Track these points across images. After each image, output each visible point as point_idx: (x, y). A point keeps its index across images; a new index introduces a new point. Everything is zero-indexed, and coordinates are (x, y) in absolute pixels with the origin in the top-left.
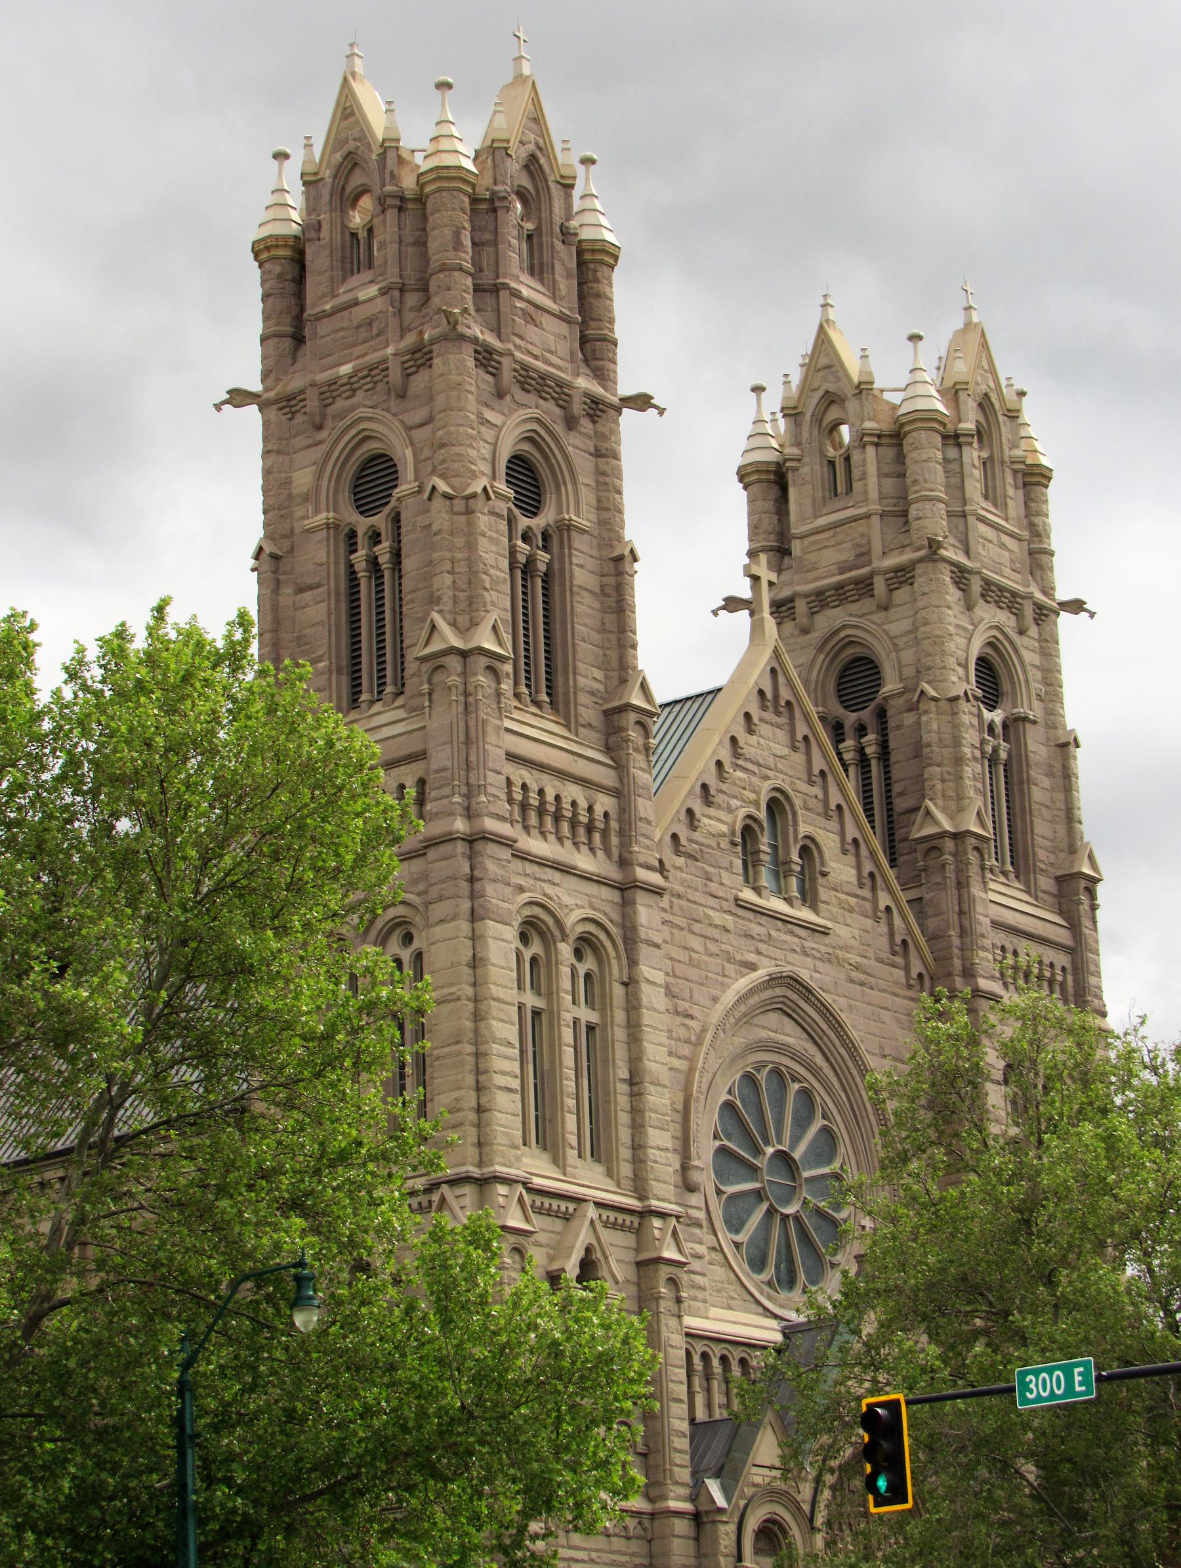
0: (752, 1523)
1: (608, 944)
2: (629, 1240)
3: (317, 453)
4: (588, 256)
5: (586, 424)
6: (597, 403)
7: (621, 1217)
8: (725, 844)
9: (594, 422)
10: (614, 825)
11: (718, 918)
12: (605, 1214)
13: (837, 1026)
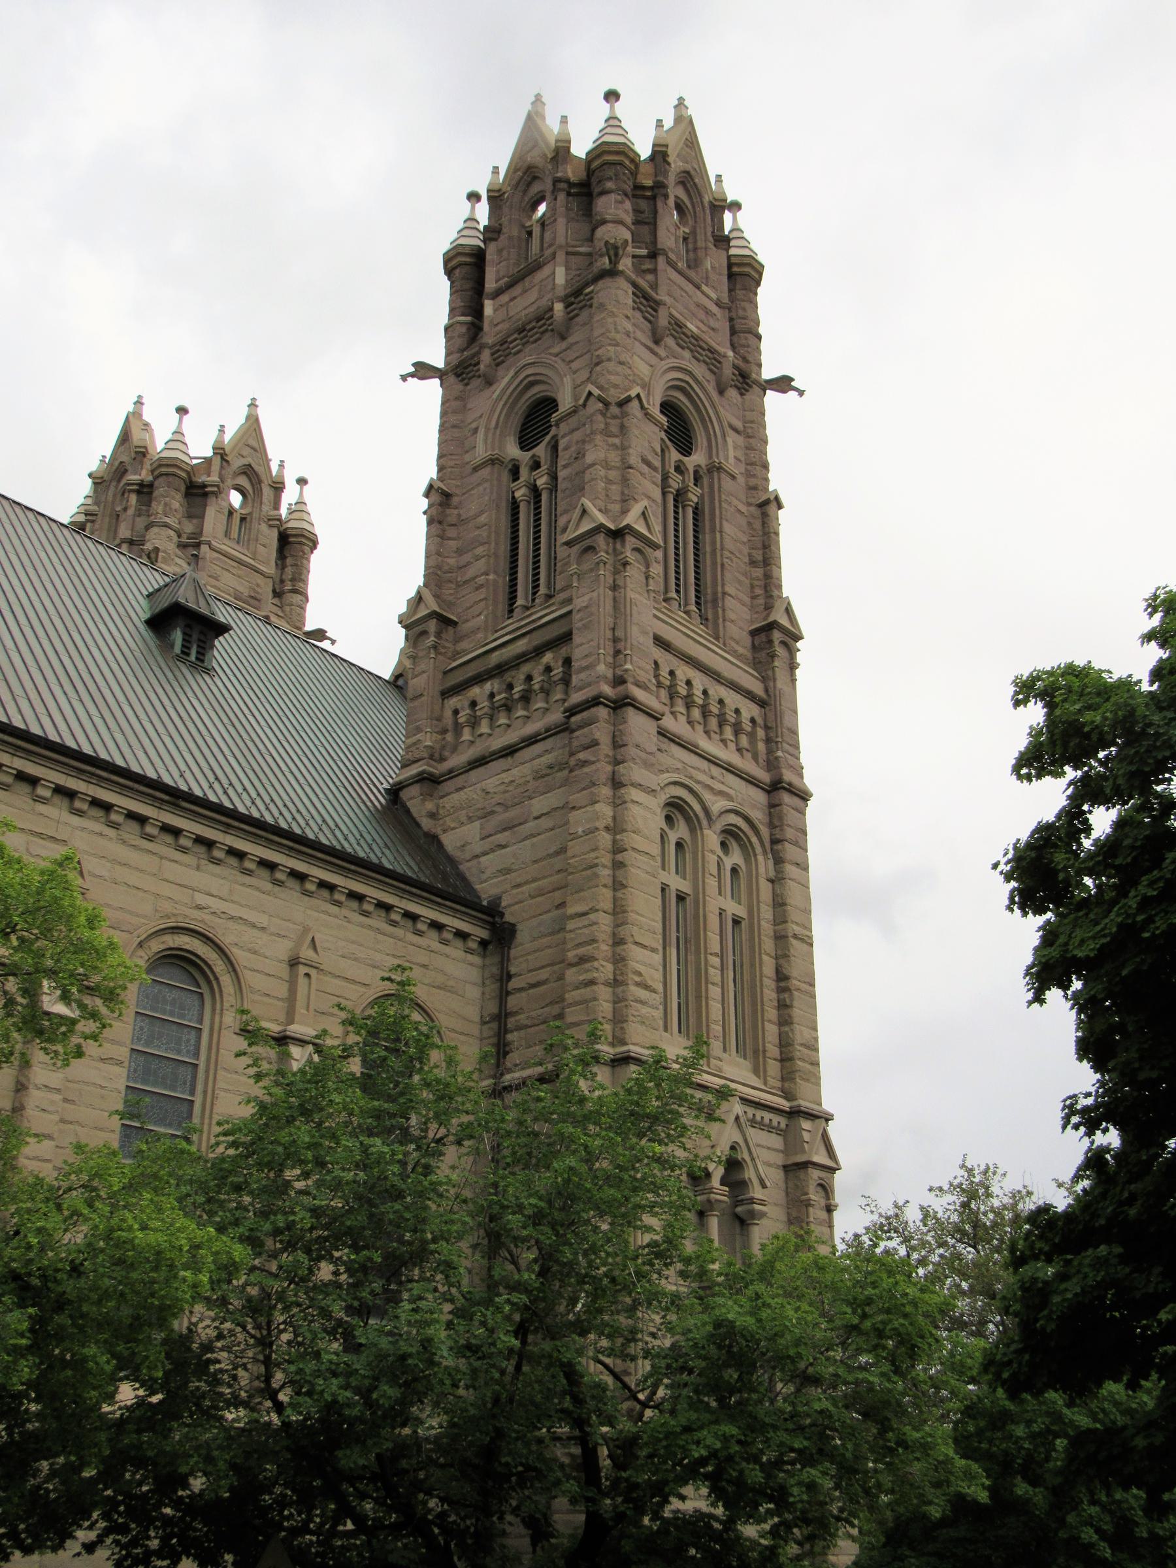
1: (754, 839)
2: (776, 1141)
4: (735, 269)
5: (732, 393)
7: (767, 1116)
9: (742, 394)
10: (761, 733)
12: (751, 1111)
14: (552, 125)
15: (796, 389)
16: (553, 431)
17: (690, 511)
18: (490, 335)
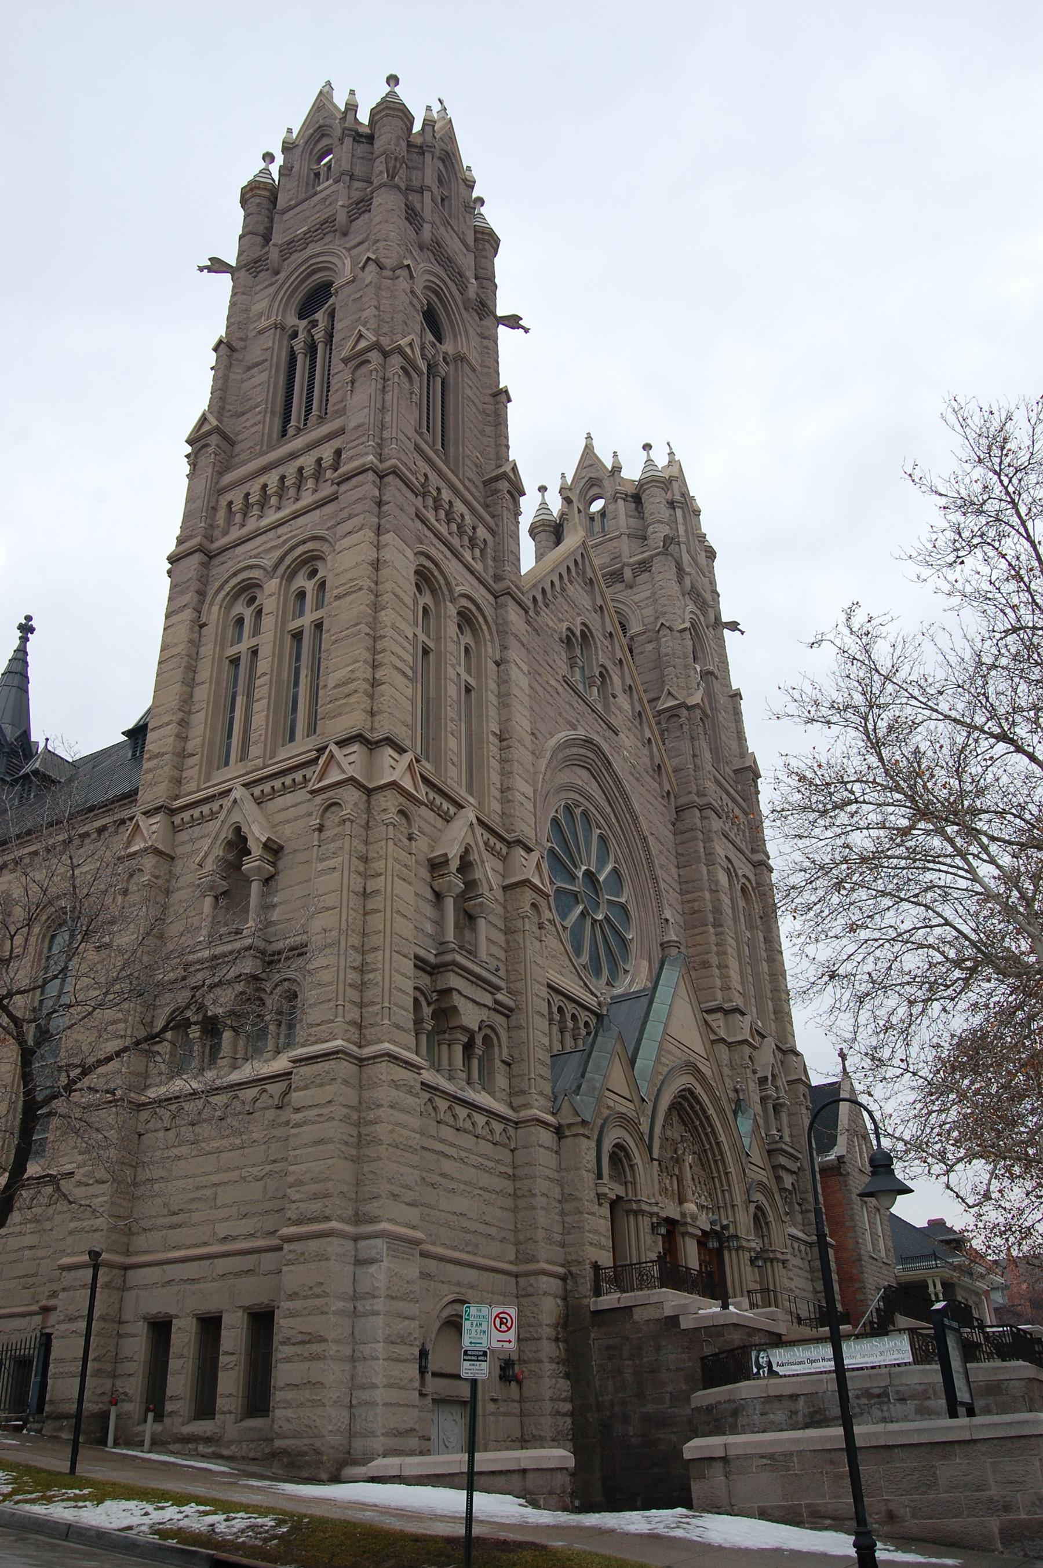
0: (607, 1147)
2: (499, 865)
3: (272, 290)
4: (479, 236)
6: (484, 306)
8: (556, 637)
11: (553, 682)
13: (626, 798)
14: (340, 101)
15: (523, 327)
16: (332, 300)
17: (439, 381)
18: (278, 237)
